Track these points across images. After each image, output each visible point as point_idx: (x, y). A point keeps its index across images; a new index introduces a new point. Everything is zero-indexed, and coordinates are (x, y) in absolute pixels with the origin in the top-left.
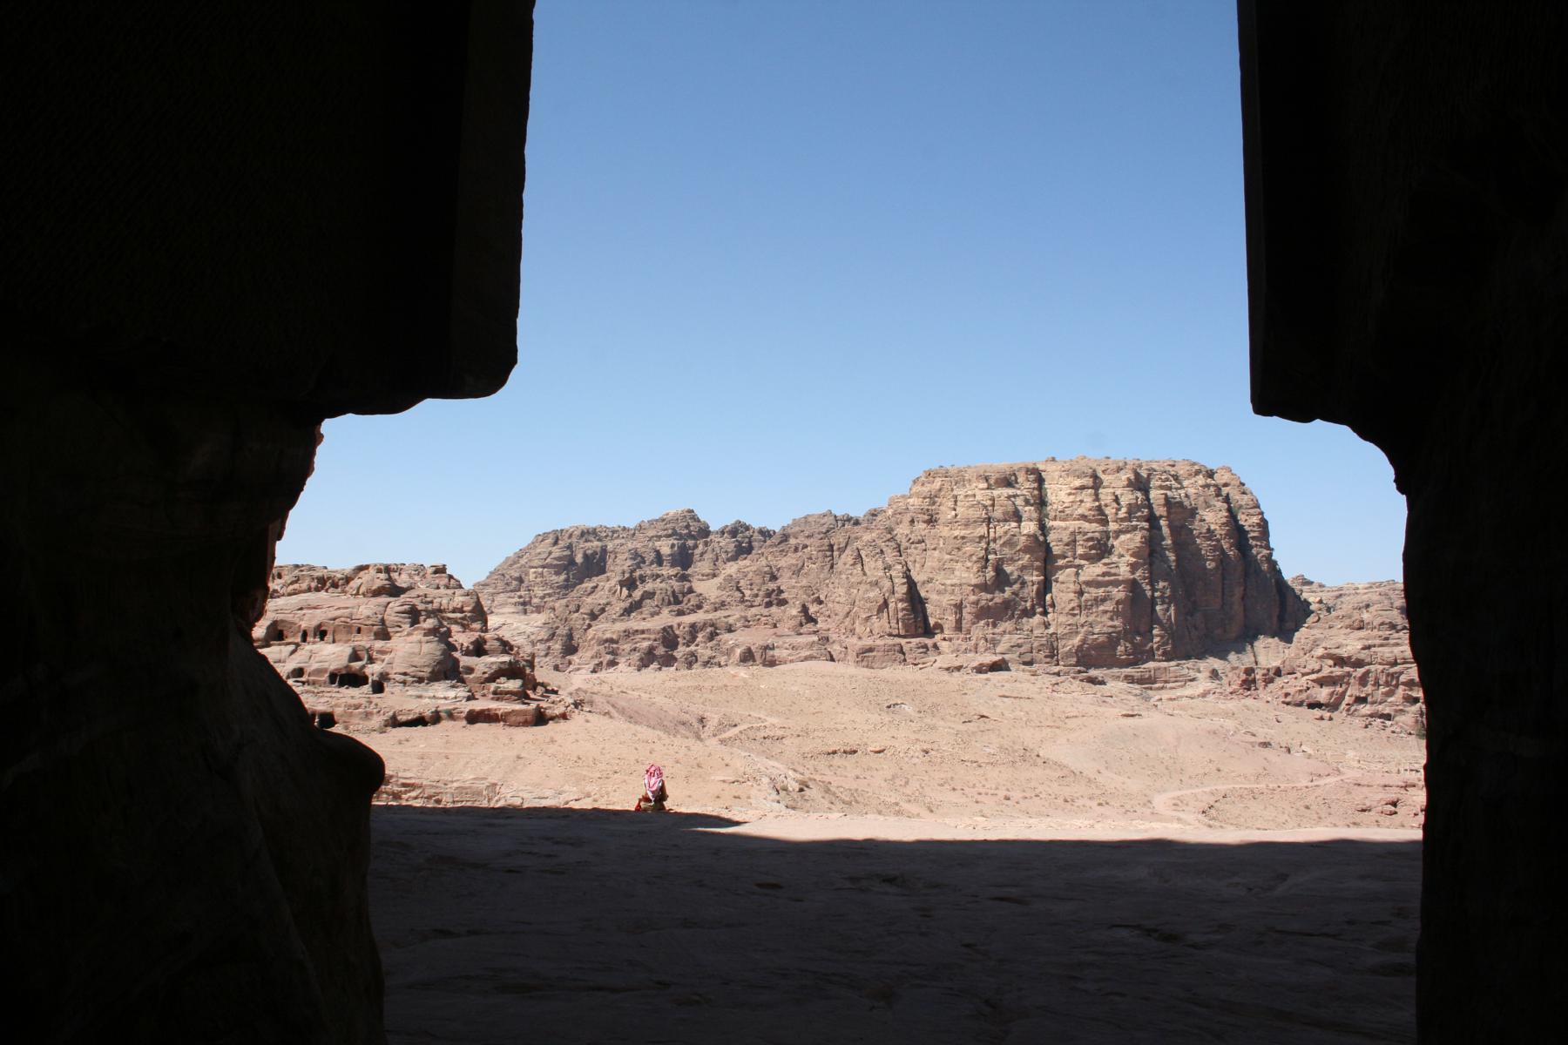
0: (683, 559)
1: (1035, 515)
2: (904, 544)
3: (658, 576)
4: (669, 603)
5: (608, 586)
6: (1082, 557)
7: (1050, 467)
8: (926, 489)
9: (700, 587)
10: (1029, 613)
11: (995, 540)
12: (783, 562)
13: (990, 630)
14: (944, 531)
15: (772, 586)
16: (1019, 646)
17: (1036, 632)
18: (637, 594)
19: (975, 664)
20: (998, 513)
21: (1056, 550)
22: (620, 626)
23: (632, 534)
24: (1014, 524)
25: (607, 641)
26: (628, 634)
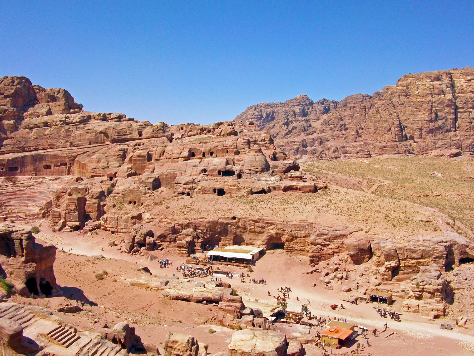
0: (304, 114)
1: (451, 92)
2: (396, 105)
3: (298, 121)
4: (303, 131)
5: (279, 125)
6: (471, 108)
7: (455, 72)
8: (405, 83)
9: (314, 124)
10: (448, 131)
11: (435, 102)
12: (345, 114)
13: (433, 138)
14: (414, 99)
15: (342, 123)
16: (445, 144)
17: (453, 139)
18: (290, 127)
19: (449, 154)
20: (436, 91)
21: (459, 105)
22: (285, 140)
23: (284, 105)
24: (443, 96)
25: (281, 146)
26: (289, 143)
